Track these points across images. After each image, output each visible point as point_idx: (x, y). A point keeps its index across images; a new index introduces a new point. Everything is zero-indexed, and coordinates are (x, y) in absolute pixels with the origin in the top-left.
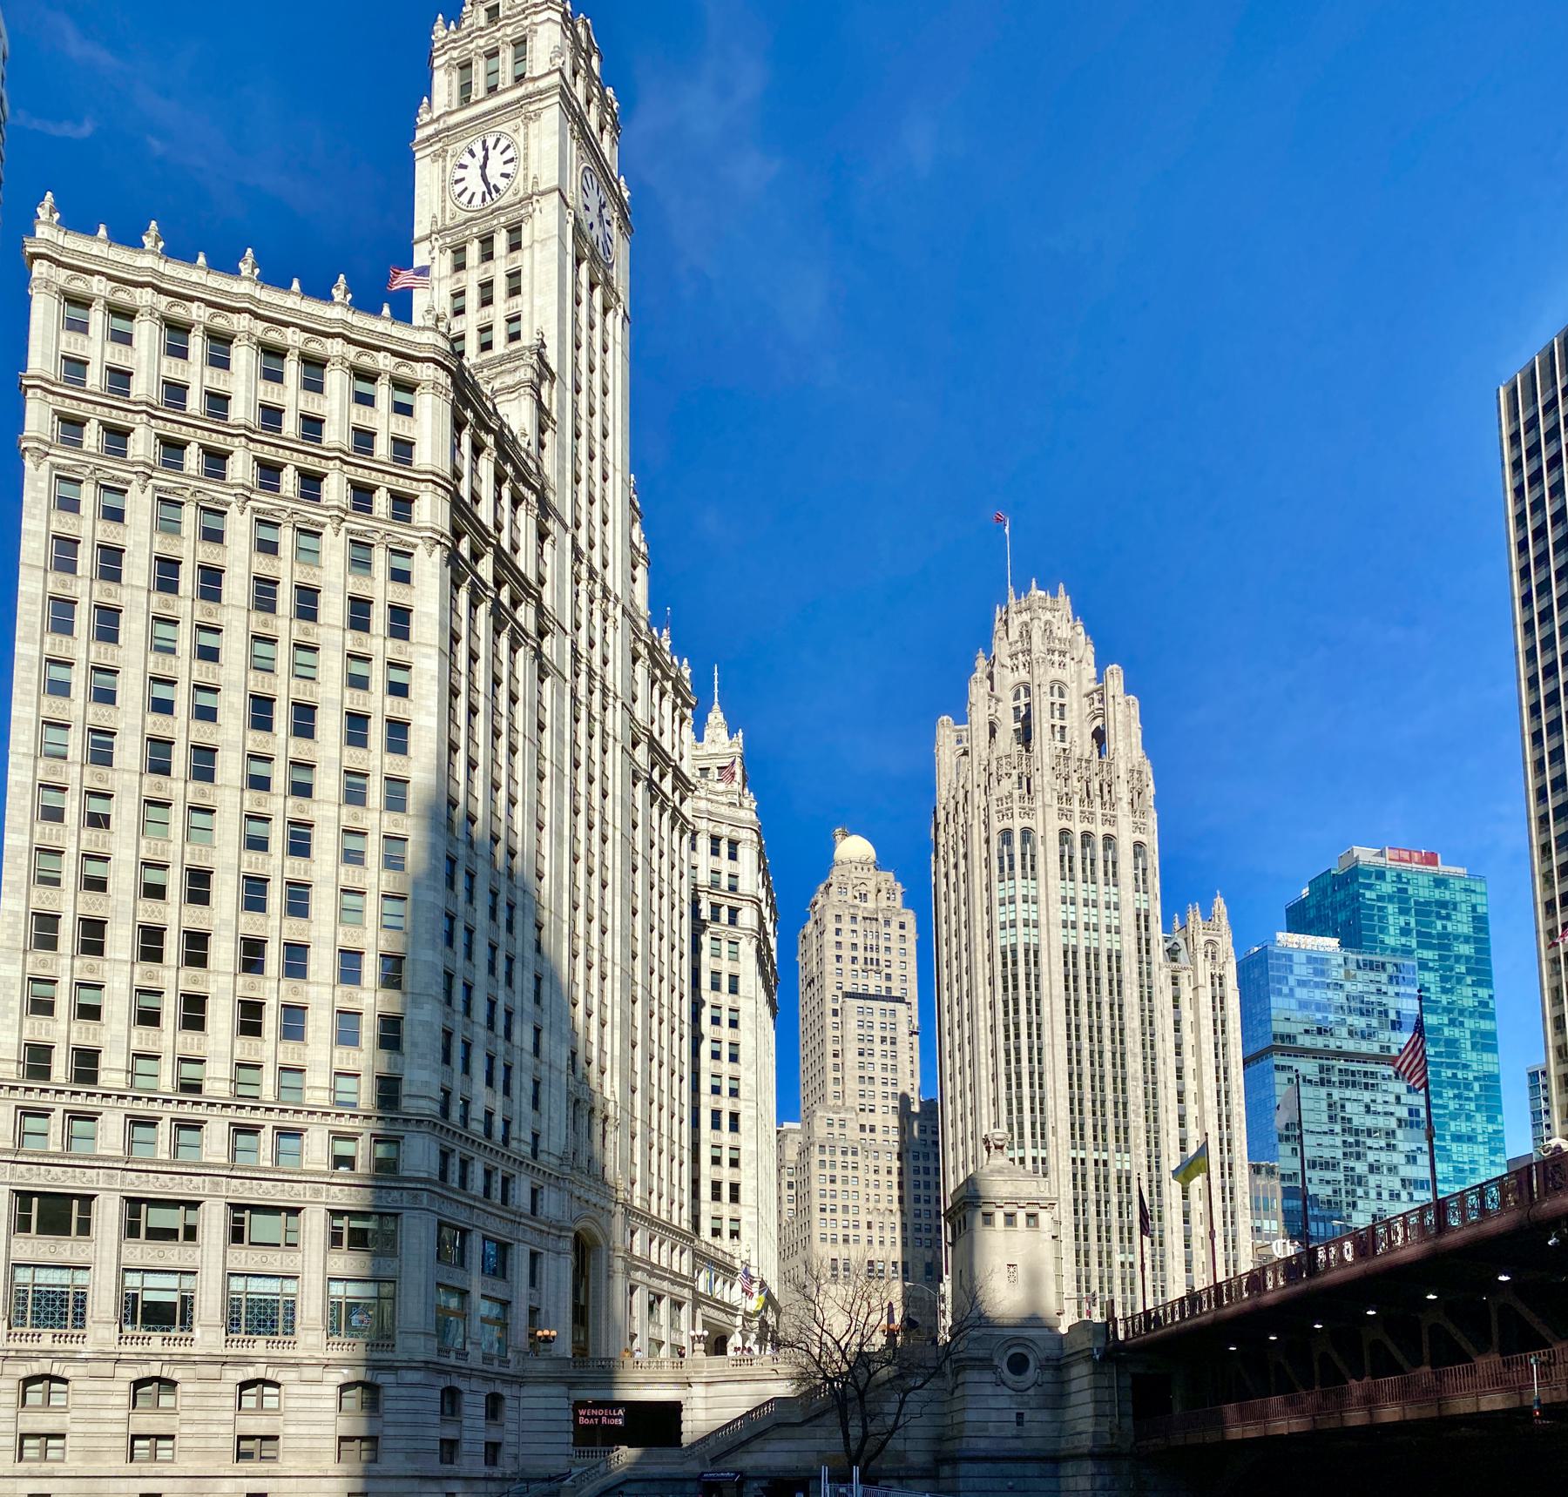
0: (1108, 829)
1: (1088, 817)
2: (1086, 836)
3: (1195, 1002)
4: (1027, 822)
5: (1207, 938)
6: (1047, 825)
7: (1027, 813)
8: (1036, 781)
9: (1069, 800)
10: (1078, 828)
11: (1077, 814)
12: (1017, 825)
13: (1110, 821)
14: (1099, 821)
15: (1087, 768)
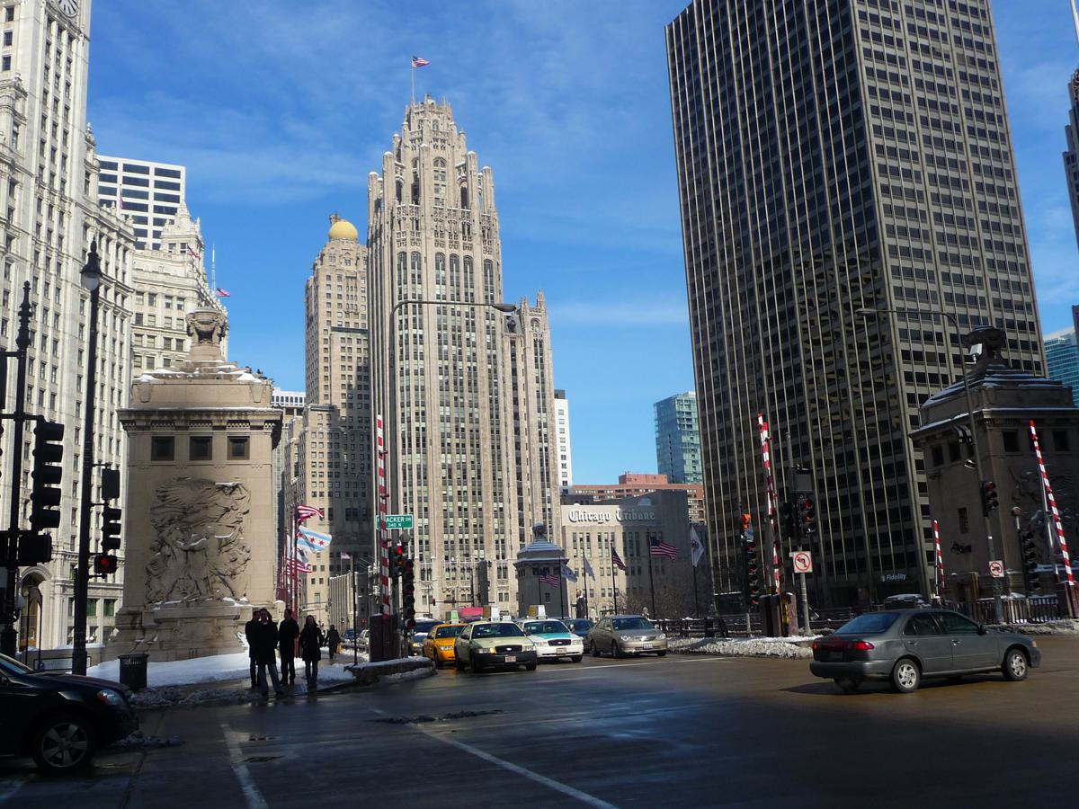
0: (467, 253)
1: (455, 245)
2: (454, 257)
3: (524, 357)
4: (415, 248)
5: (532, 317)
6: (429, 250)
7: (414, 242)
8: (422, 224)
9: (442, 234)
10: (448, 252)
11: (447, 244)
12: (410, 249)
13: (470, 248)
14: (461, 248)
15: (455, 215)
